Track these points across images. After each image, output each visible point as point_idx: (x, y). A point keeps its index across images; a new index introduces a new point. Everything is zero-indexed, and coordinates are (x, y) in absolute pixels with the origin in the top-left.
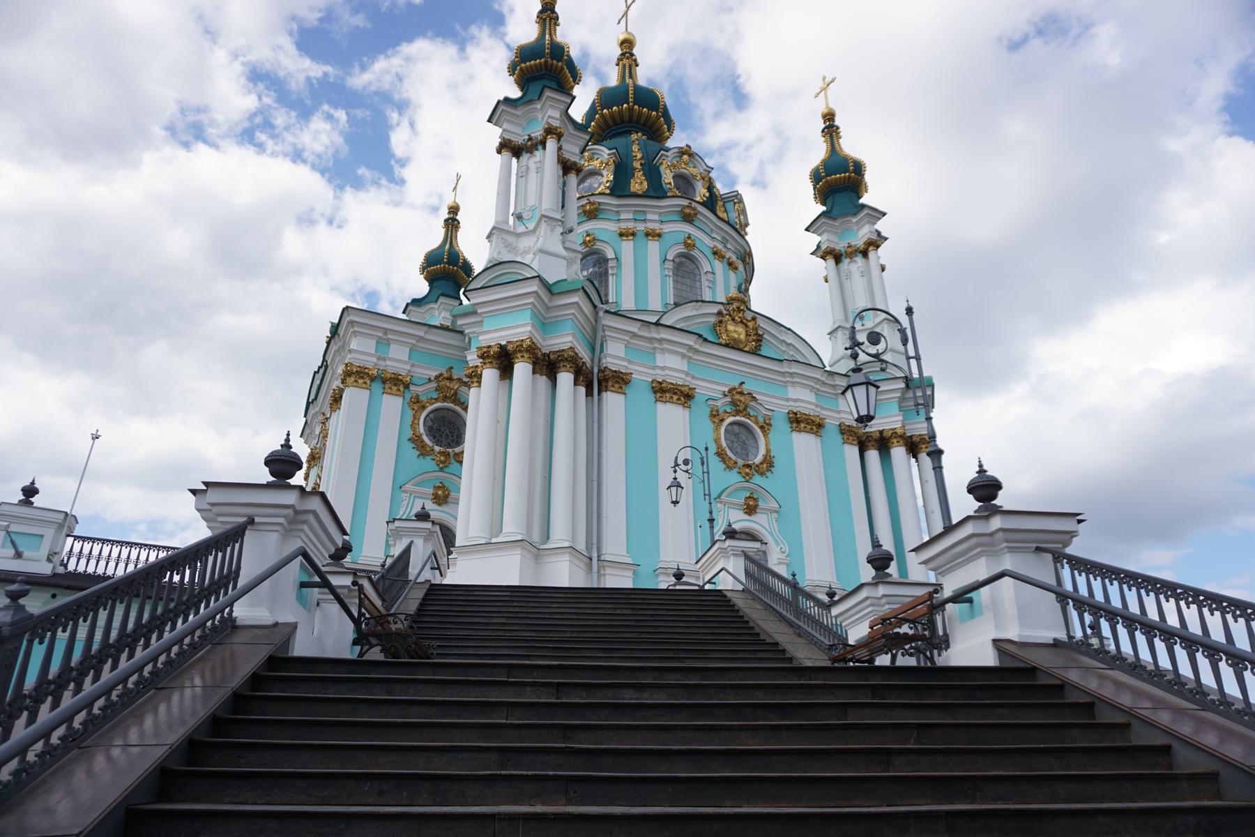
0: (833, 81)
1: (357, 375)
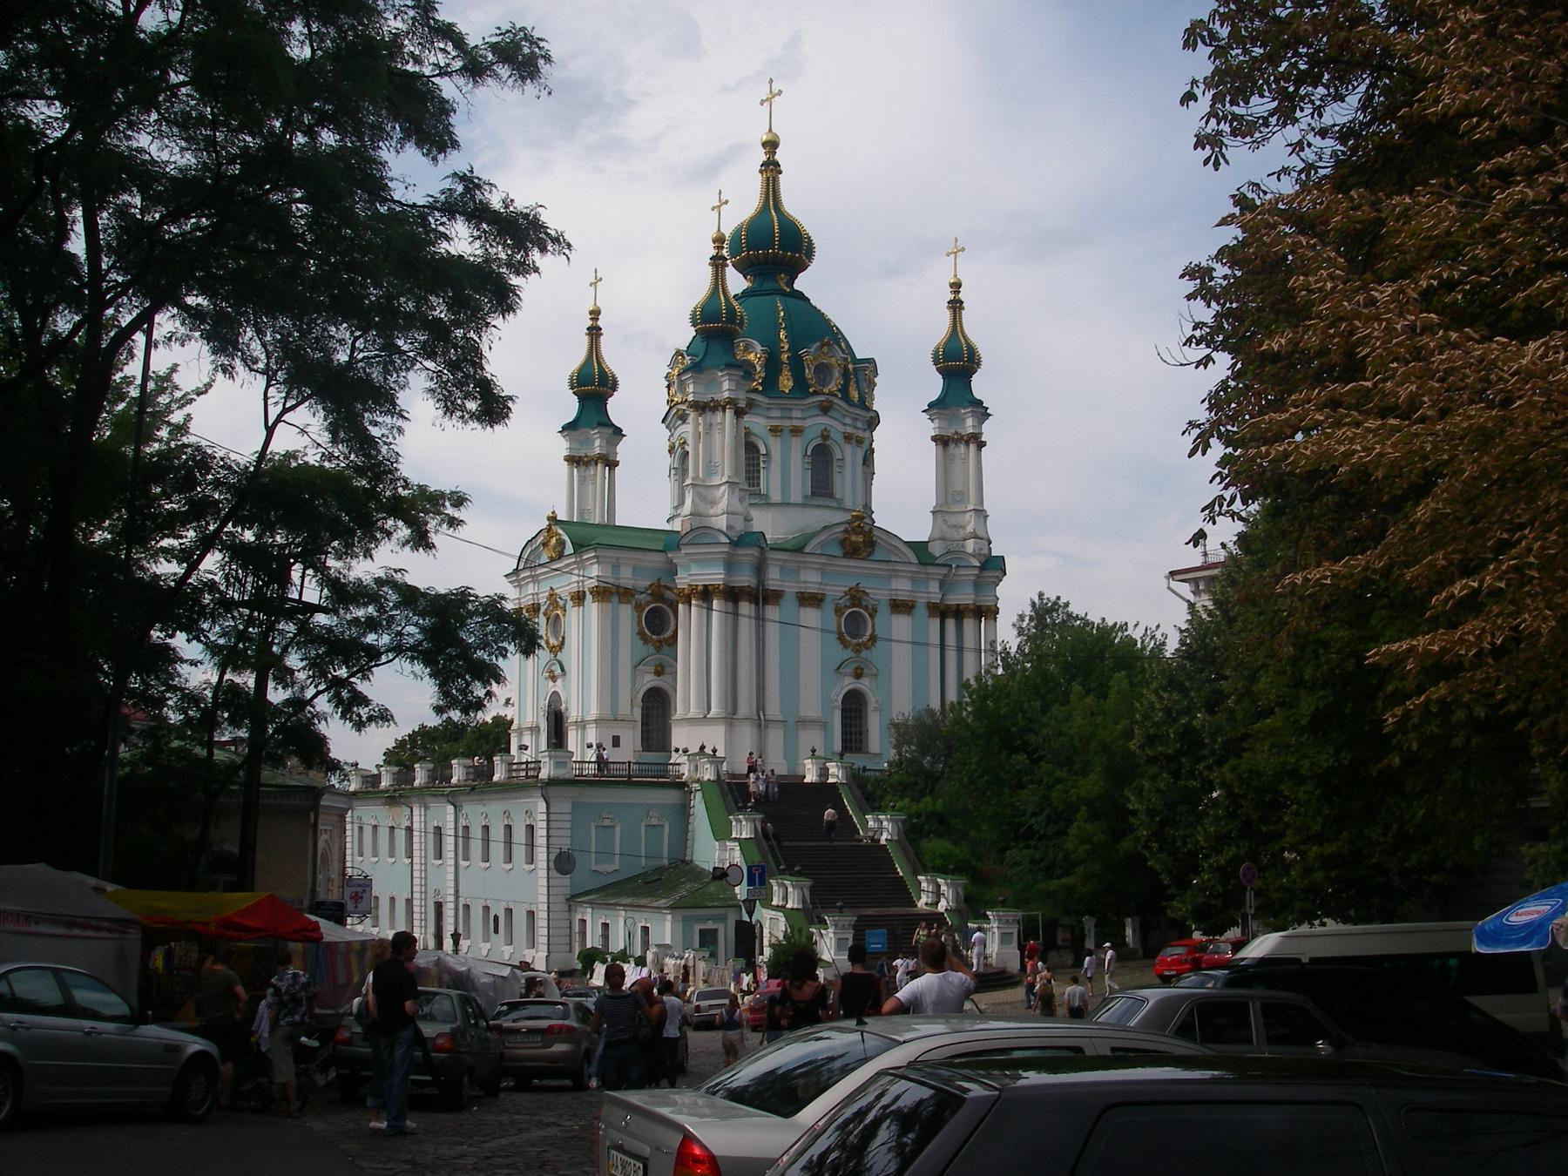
0: (963, 249)
1: (603, 593)
